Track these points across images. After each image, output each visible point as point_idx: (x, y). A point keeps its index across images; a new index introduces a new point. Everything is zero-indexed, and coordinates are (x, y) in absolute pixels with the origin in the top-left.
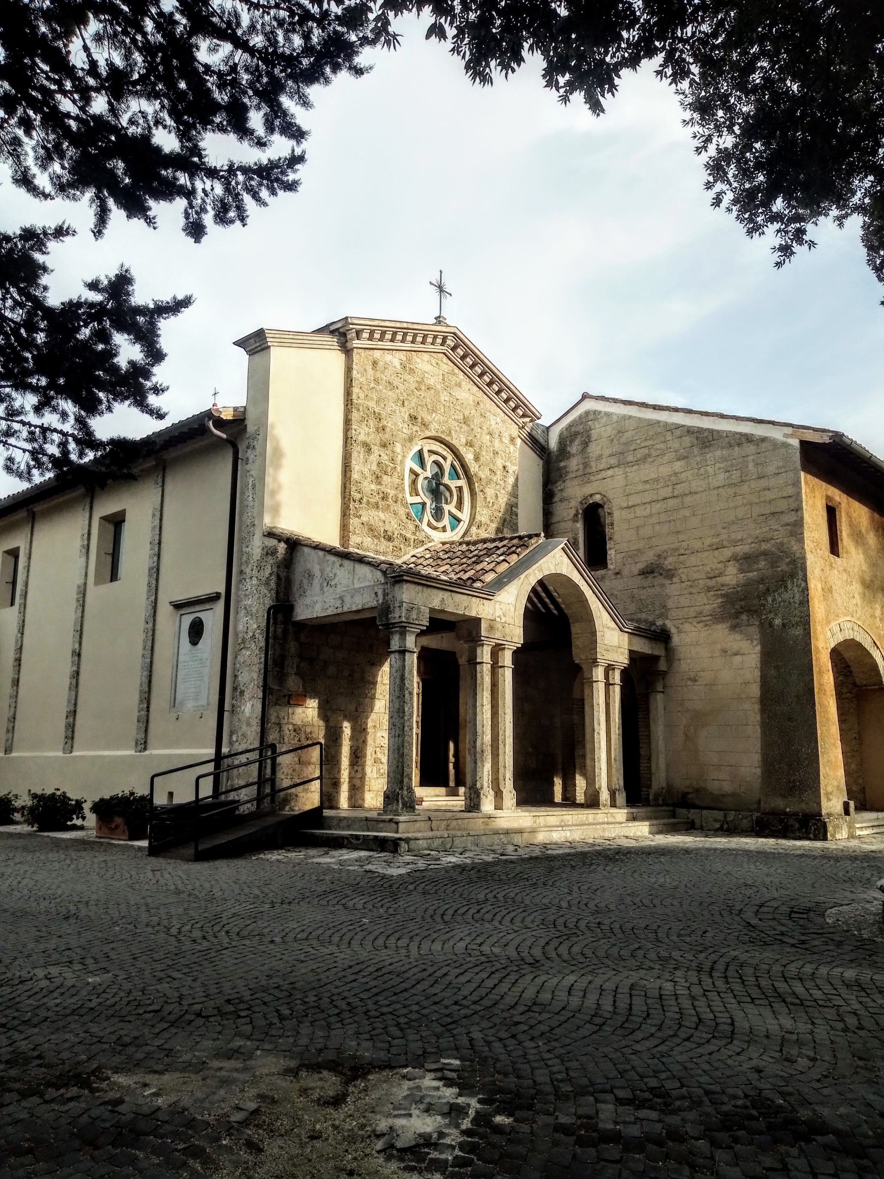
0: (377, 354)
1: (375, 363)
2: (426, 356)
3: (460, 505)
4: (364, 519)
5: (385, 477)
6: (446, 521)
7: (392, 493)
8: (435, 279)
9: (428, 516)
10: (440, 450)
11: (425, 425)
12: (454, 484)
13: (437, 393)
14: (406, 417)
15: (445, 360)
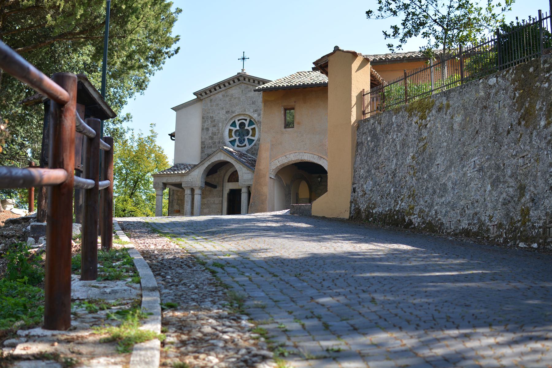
0: (212, 97)
1: (211, 100)
2: (233, 88)
3: (253, 135)
4: (206, 153)
5: (215, 136)
6: (246, 142)
9: (237, 143)
10: (243, 118)
14: (224, 113)
15: (243, 85)
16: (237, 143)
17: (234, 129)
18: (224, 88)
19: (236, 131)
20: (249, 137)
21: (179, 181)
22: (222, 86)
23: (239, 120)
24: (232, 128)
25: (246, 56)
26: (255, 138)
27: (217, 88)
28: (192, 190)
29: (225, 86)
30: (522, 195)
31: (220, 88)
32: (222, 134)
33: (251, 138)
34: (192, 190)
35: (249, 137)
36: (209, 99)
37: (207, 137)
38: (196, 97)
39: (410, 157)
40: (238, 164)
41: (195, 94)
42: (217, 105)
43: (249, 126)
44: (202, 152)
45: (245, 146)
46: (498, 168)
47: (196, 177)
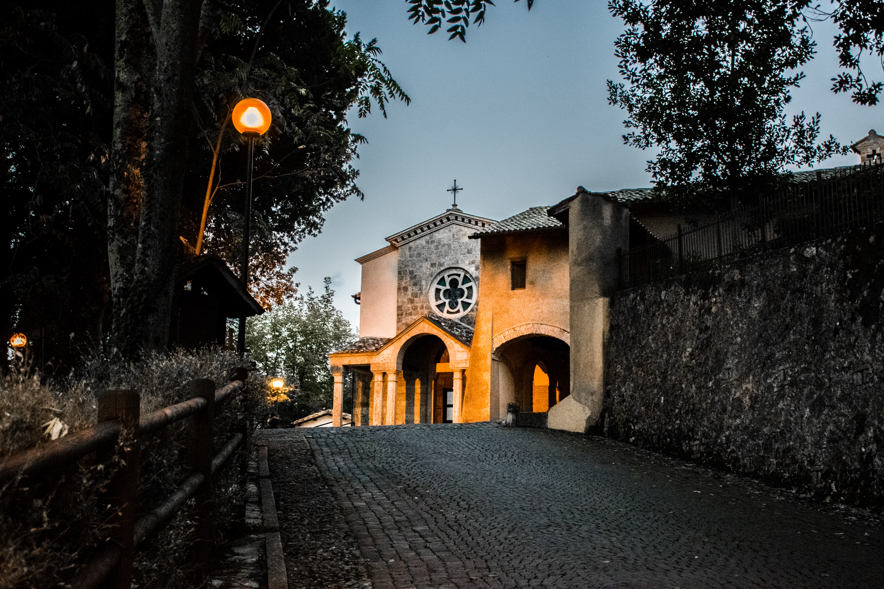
0: (411, 244)
1: (410, 248)
3: (470, 296)
4: (404, 322)
6: (460, 307)
7: (419, 305)
8: (451, 186)
9: (447, 308)
11: (441, 265)
12: (464, 287)
13: (449, 245)
15: (454, 226)
16: (447, 308)
17: (443, 288)
18: (428, 232)
19: (445, 291)
20: (464, 299)
21: (366, 362)
22: (425, 229)
23: (449, 276)
24: (440, 287)
25: (459, 185)
26: (472, 301)
27: (419, 231)
28: (384, 374)
29: (429, 228)
30: (861, 430)
31: (423, 231)
32: (427, 295)
33: (466, 300)
34: (384, 374)
35: (464, 299)
36: (407, 246)
37: (405, 300)
38: (389, 244)
39: (687, 354)
40: (448, 339)
41: (387, 239)
42: (419, 254)
43: (463, 284)
44: (399, 321)
45: (458, 311)
46: (820, 385)
47: (388, 359)
